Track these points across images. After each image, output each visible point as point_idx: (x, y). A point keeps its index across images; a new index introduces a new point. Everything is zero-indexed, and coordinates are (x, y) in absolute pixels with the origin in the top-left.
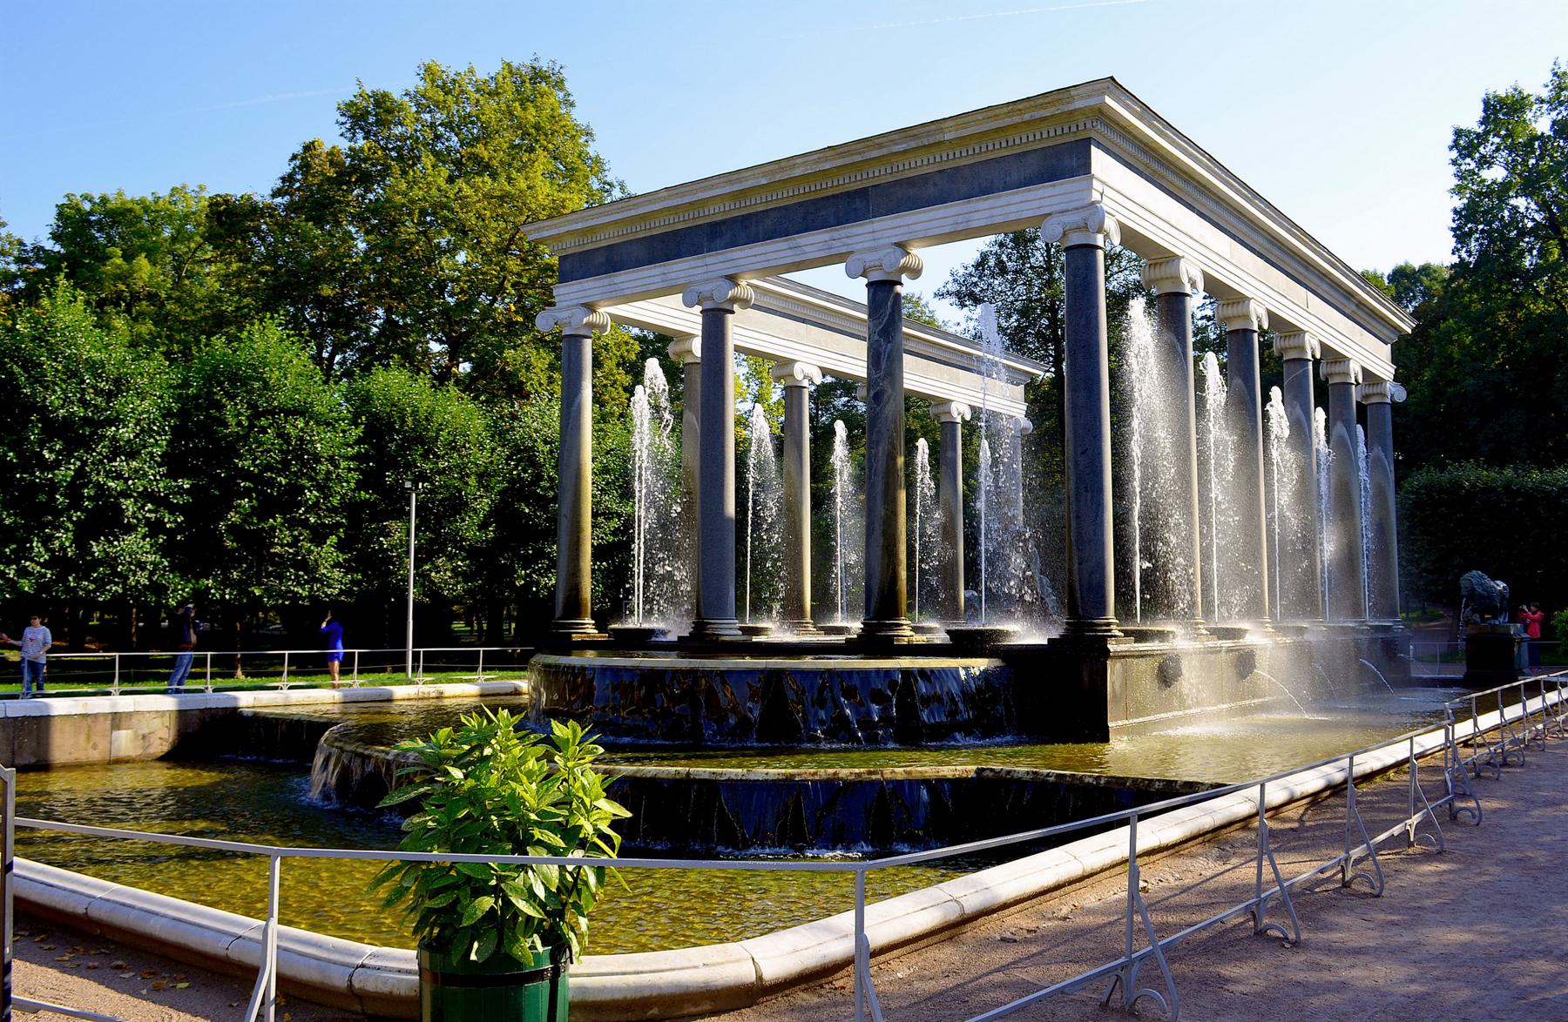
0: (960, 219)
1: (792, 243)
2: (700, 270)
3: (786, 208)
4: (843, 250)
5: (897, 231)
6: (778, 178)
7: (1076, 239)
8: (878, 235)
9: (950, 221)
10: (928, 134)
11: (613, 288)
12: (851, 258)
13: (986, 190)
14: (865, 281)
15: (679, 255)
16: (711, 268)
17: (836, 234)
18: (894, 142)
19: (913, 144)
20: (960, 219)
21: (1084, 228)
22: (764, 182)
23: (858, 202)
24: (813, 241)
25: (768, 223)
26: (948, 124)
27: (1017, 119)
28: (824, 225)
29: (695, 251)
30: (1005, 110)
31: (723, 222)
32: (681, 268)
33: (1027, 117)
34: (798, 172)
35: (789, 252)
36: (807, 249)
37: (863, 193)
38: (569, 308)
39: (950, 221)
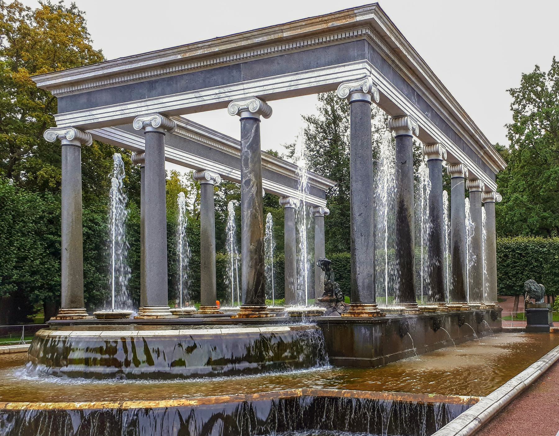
0: (292, 83)
1: (197, 95)
2: (144, 109)
3: (193, 74)
4: (227, 99)
5: (257, 89)
7: (356, 97)
8: (246, 91)
9: (287, 84)
10: (275, 32)
11: (92, 117)
12: (231, 105)
13: (307, 67)
14: (240, 118)
16: (150, 107)
17: (222, 90)
18: (255, 37)
19: (266, 38)
20: (292, 83)
21: (361, 91)
23: (235, 71)
24: (209, 95)
25: (183, 83)
26: (285, 27)
27: (324, 26)
29: (141, 97)
30: (318, 20)
33: (330, 25)
34: (200, 52)
35: (195, 100)
36: (205, 98)
38: (65, 128)
39: (287, 84)
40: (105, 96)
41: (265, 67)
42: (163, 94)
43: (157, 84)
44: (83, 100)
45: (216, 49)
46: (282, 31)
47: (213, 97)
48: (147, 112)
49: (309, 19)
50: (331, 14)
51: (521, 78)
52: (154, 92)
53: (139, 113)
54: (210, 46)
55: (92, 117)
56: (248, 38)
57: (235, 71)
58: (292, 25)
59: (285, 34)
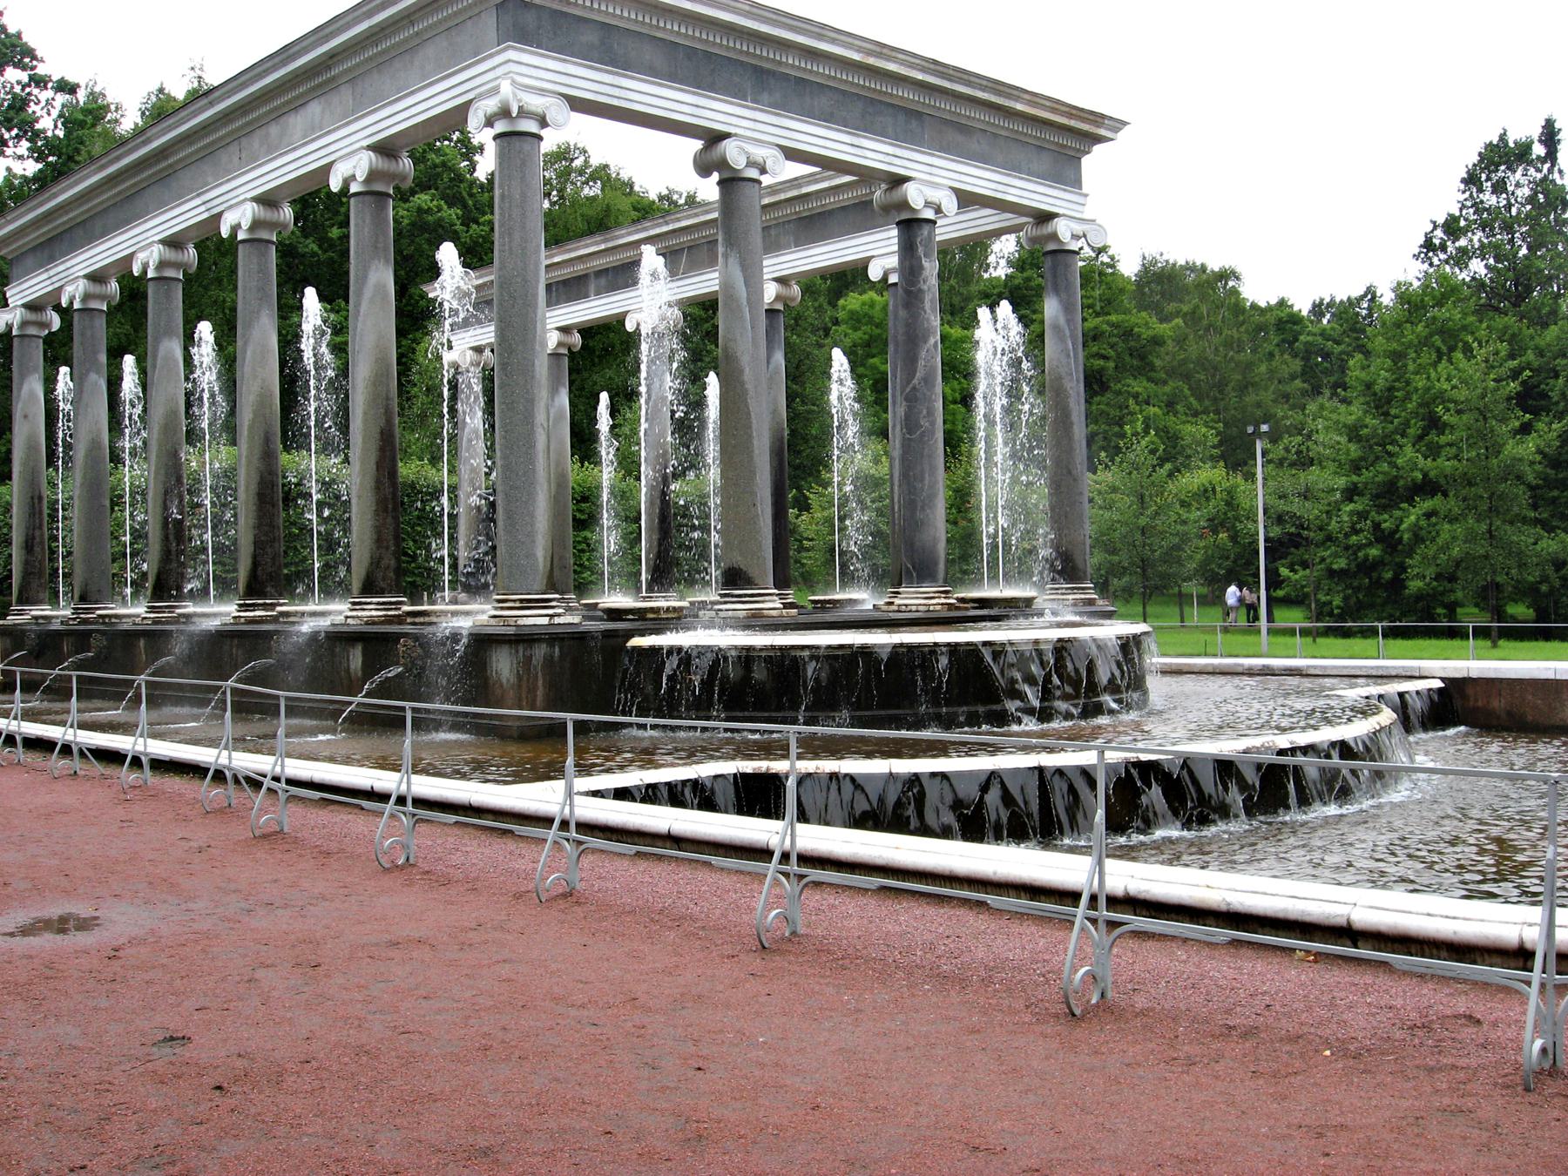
3: (844, 93)
6: (871, 61)
9: (993, 186)
11: (617, 92)
13: (1012, 167)
15: (712, 87)
17: (898, 152)
20: (1001, 188)
22: (856, 56)
25: (823, 102)
28: (880, 133)
29: (735, 92)
31: (772, 73)
32: (717, 111)
33: (1073, 123)
34: (892, 67)
37: (918, 115)
39: (993, 186)
40: (649, 54)
41: (960, 138)
42: (782, 106)
43: (772, 81)
44: (590, 37)
45: (920, 76)
46: (1017, 99)
47: (881, 157)
48: (749, 133)
49: (1058, 102)
50: (1082, 110)
51: (154, 87)
52: (765, 97)
53: (732, 130)
54: (912, 66)
55: (617, 92)
56: (969, 84)
57: (914, 124)
58: (1035, 98)
59: (1019, 107)
